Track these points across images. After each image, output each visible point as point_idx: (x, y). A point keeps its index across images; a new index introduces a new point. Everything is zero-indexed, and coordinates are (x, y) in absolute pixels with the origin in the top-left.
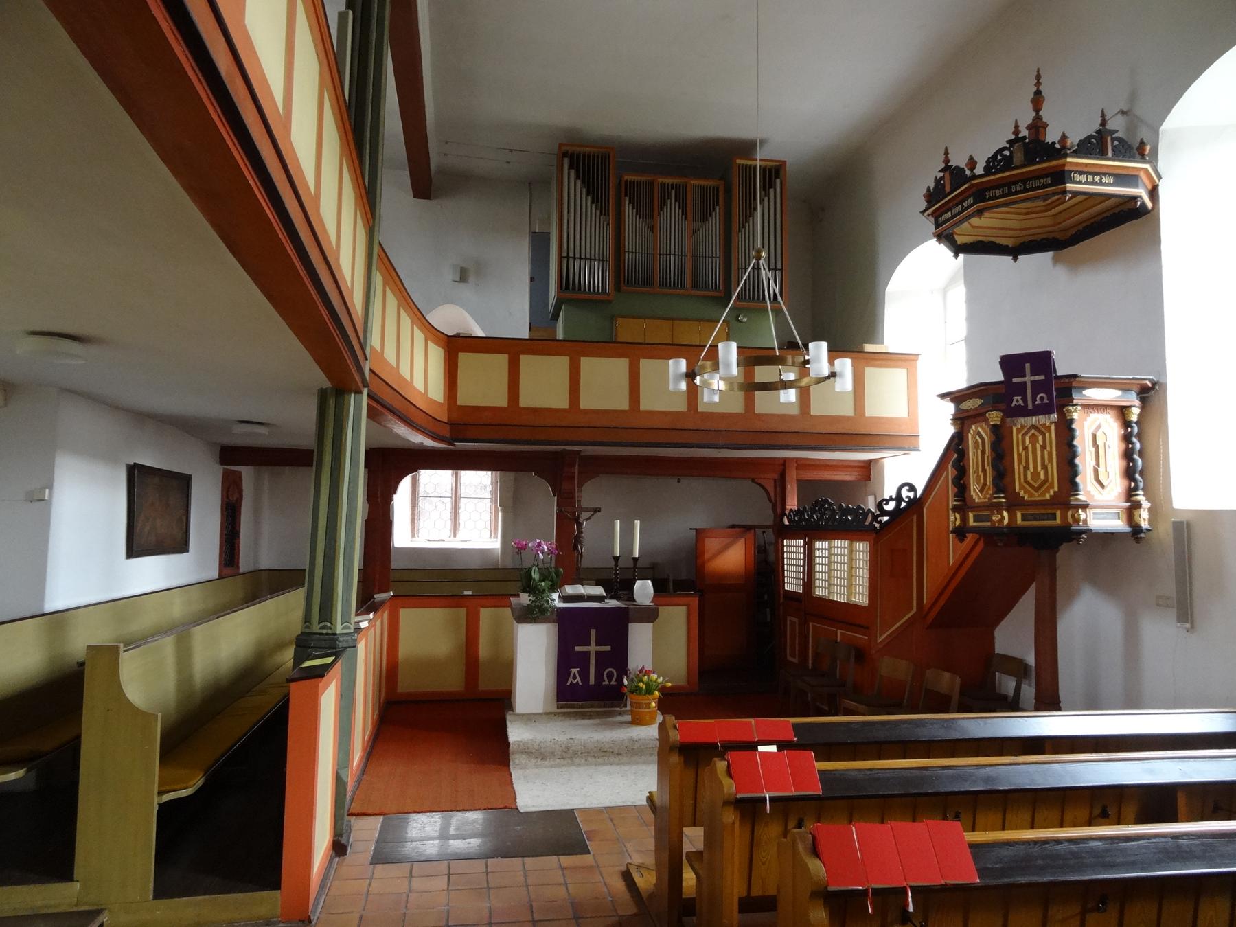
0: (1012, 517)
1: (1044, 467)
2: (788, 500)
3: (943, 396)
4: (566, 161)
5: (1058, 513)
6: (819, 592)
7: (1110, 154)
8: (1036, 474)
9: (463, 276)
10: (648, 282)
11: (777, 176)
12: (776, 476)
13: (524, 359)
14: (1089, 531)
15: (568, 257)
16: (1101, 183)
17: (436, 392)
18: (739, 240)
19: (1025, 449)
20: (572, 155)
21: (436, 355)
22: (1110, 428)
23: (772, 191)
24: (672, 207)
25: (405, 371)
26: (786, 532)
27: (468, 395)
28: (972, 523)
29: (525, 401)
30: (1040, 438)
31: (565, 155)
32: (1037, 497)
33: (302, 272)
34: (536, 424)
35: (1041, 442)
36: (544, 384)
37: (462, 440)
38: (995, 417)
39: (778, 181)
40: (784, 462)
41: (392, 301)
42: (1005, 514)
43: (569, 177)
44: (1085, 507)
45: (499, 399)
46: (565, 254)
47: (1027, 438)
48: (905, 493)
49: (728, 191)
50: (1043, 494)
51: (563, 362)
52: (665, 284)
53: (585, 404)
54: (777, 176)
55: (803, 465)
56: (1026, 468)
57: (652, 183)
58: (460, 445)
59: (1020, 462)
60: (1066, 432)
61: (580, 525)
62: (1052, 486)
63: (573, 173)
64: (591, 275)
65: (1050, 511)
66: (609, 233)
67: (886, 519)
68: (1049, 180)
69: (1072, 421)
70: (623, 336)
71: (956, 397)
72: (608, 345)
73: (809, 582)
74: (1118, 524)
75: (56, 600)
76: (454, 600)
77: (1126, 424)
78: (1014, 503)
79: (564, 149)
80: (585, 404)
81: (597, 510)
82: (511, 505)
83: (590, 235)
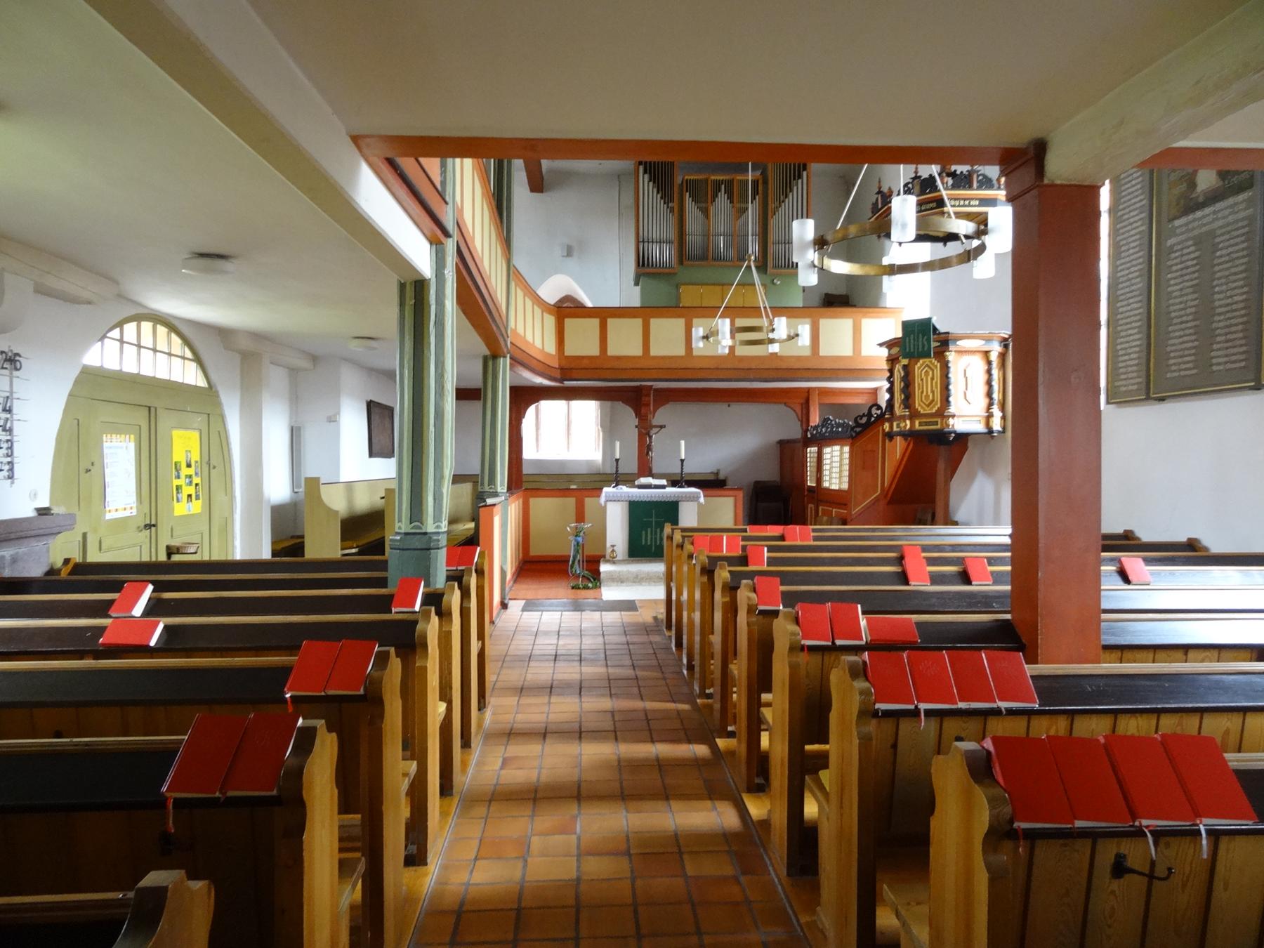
0: (912, 424)
1: (933, 392)
2: (811, 419)
3: (881, 345)
4: (641, 169)
6: (826, 484)
7: (975, 185)
8: (927, 396)
9: (569, 252)
11: (805, 169)
12: (803, 401)
13: (609, 321)
14: (955, 432)
16: (969, 206)
17: (551, 348)
18: (773, 223)
21: (550, 321)
22: (978, 365)
24: (722, 198)
25: (529, 338)
26: (807, 442)
27: (571, 350)
28: (895, 429)
29: (612, 351)
32: (928, 411)
33: (470, 283)
34: (619, 367)
36: (625, 341)
37: (570, 380)
38: (905, 362)
39: (805, 173)
40: (808, 391)
41: (520, 293)
42: (908, 422)
43: (644, 179)
44: (953, 416)
45: (594, 351)
48: (874, 411)
49: (765, 182)
51: (638, 322)
53: (654, 352)
54: (805, 169)
55: (824, 392)
57: (706, 180)
58: (567, 383)
60: (945, 367)
61: (650, 437)
63: (646, 176)
64: (663, 253)
66: (673, 219)
67: (858, 430)
68: (934, 205)
69: (948, 362)
70: (685, 302)
71: (890, 344)
72: (673, 309)
73: (819, 480)
74: (980, 427)
75: (344, 477)
76: (564, 492)
77: (989, 363)
78: (914, 415)
80: (654, 352)
81: (662, 427)
82: (609, 428)
83: (660, 225)
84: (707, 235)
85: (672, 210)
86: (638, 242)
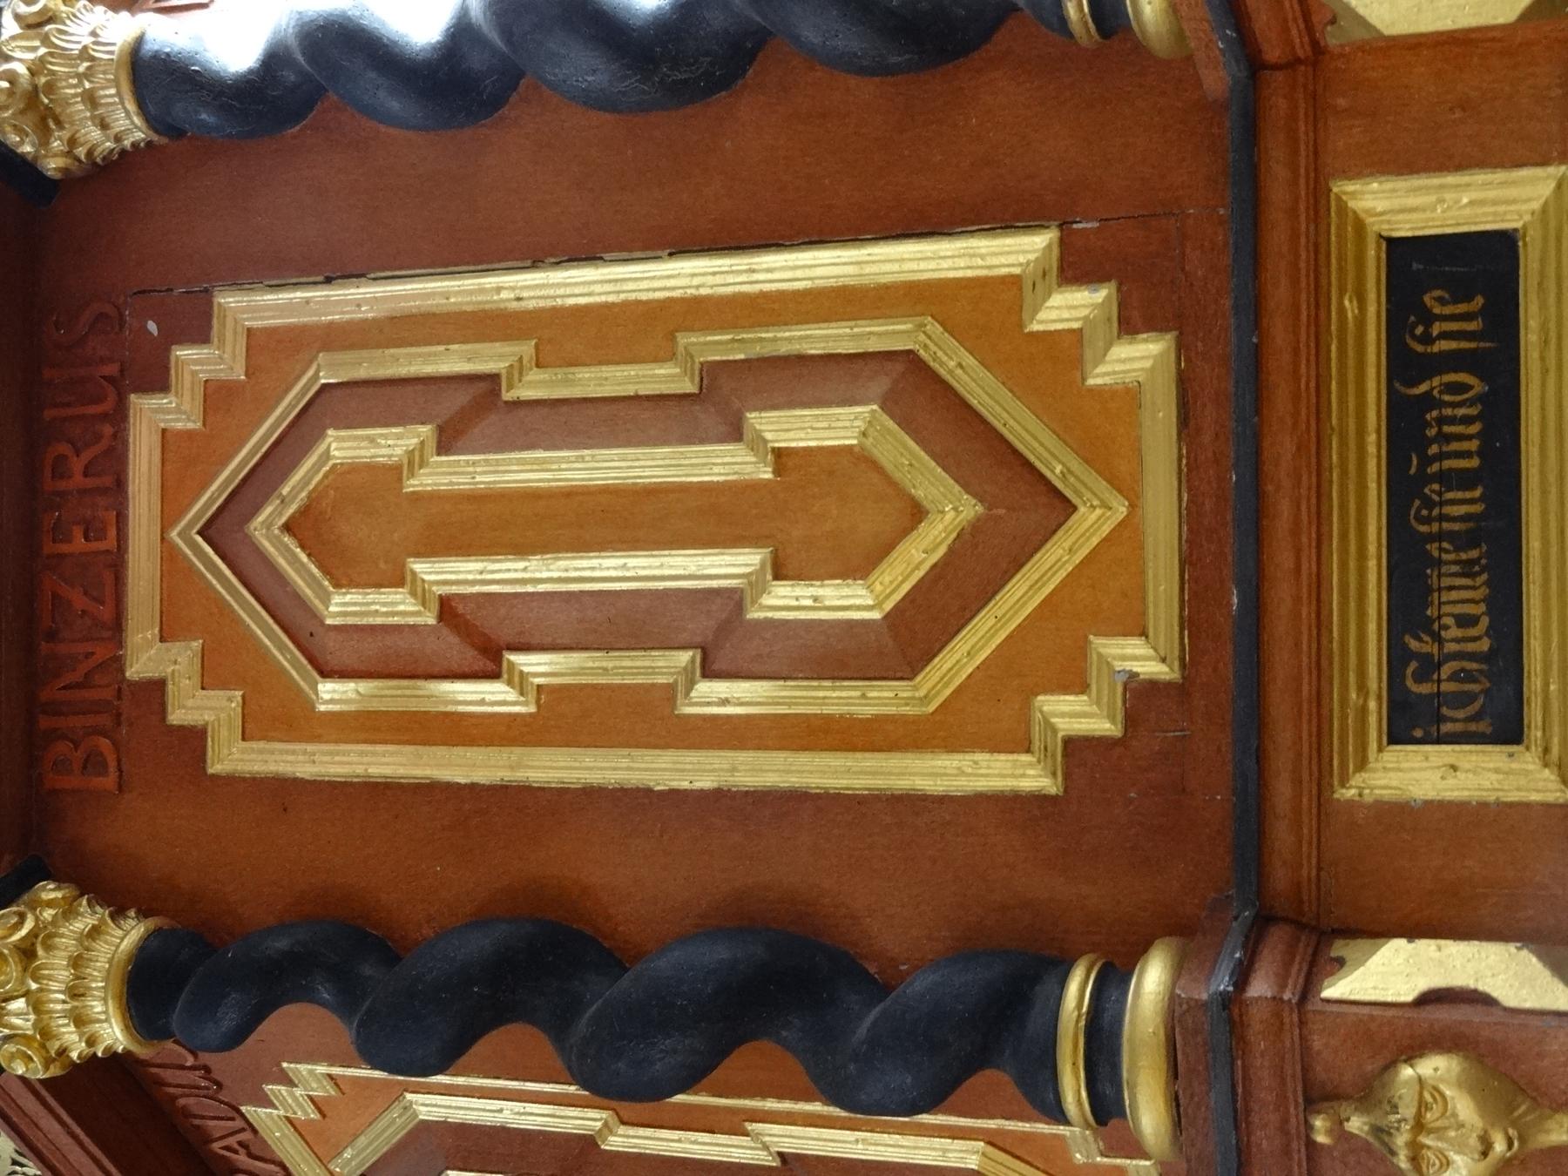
1: (717, 403)
5: (1399, 203)
8: (803, 515)
19: (480, 636)
30: (342, 447)
32: (1128, 513)
35: (390, 444)
42: (1388, 973)
47: (343, 606)
50: (1100, 427)
56: (722, 635)
59: (649, 718)
62: (986, 309)
65: (1363, 311)
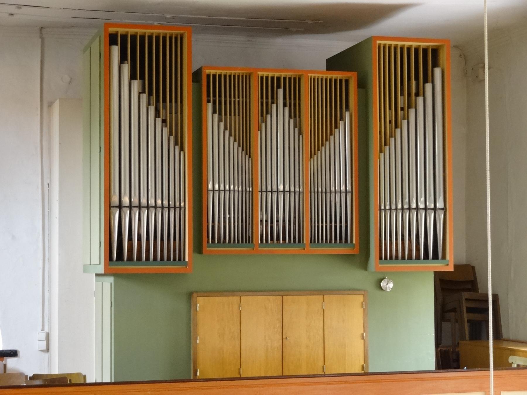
4: (116, 50)
10: (245, 238)
15: (120, 207)
20: (124, 37)
23: (429, 87)
24: (279, 114)
31: (113, 39)
39: (438, 72)
43: (120, 72)
46: (115, 200)
49: (363, 84)
52: (270, 238)
54: (435, 64)
63: (126, 68)
79: (112, 30)
84: (249, 197)
85: (179, 143)
86: (109, 207)
